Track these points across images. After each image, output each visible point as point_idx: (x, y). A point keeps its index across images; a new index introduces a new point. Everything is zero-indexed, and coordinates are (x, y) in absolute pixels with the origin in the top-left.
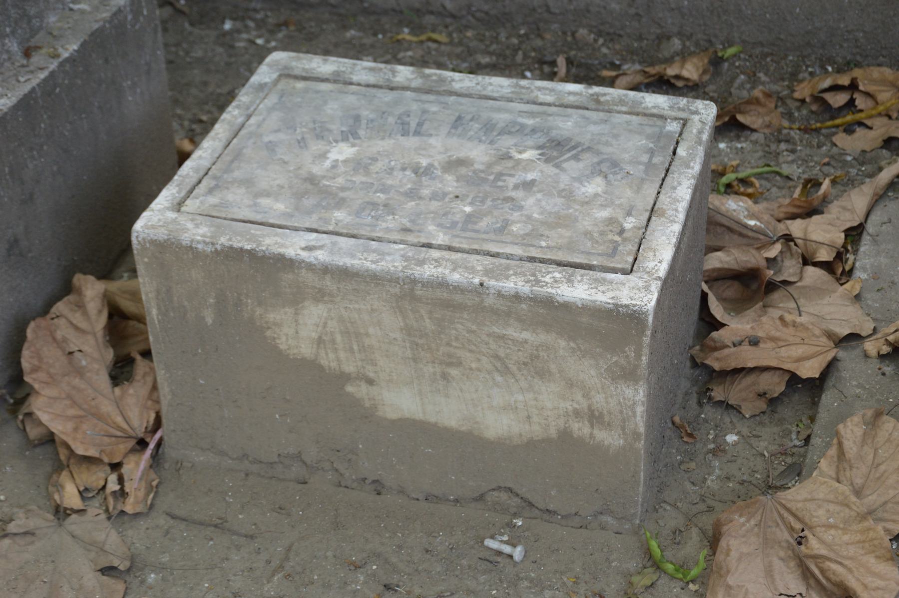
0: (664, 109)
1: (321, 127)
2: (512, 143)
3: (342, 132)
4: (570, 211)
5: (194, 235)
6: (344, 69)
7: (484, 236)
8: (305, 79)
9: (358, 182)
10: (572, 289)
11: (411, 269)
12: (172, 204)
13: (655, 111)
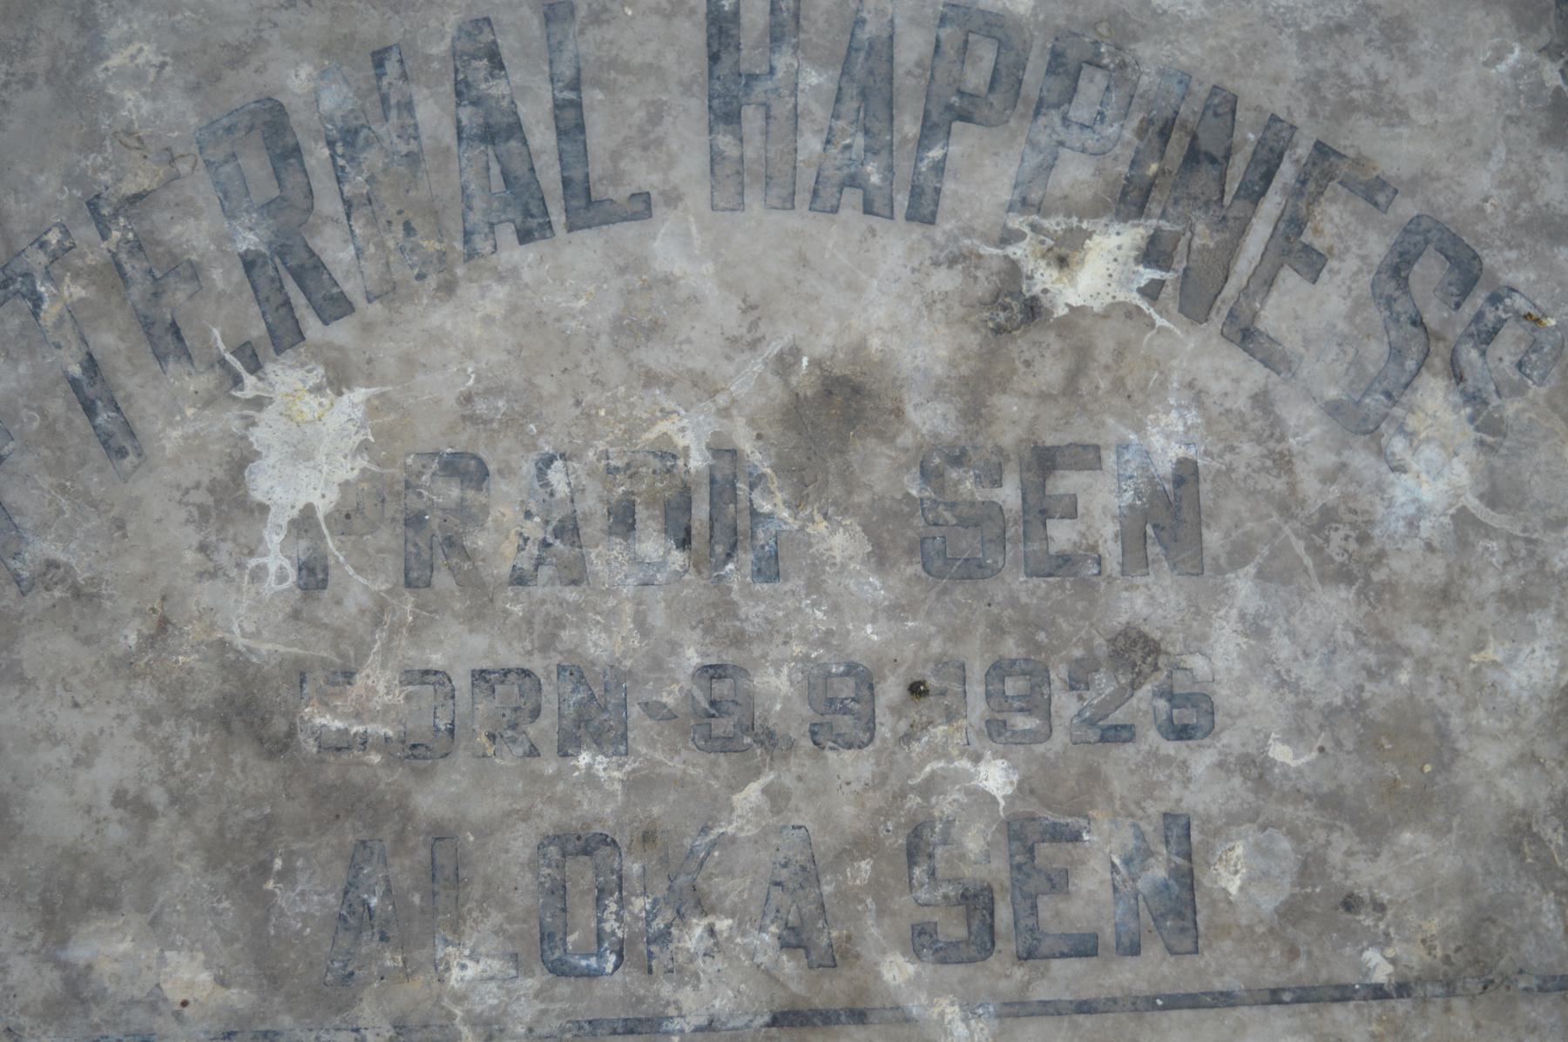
1: (137, 247)
2: (1006, 195)
3: (250, 263)
4: (1404, 678)
7: (1127, 976)
9: (462, 683)
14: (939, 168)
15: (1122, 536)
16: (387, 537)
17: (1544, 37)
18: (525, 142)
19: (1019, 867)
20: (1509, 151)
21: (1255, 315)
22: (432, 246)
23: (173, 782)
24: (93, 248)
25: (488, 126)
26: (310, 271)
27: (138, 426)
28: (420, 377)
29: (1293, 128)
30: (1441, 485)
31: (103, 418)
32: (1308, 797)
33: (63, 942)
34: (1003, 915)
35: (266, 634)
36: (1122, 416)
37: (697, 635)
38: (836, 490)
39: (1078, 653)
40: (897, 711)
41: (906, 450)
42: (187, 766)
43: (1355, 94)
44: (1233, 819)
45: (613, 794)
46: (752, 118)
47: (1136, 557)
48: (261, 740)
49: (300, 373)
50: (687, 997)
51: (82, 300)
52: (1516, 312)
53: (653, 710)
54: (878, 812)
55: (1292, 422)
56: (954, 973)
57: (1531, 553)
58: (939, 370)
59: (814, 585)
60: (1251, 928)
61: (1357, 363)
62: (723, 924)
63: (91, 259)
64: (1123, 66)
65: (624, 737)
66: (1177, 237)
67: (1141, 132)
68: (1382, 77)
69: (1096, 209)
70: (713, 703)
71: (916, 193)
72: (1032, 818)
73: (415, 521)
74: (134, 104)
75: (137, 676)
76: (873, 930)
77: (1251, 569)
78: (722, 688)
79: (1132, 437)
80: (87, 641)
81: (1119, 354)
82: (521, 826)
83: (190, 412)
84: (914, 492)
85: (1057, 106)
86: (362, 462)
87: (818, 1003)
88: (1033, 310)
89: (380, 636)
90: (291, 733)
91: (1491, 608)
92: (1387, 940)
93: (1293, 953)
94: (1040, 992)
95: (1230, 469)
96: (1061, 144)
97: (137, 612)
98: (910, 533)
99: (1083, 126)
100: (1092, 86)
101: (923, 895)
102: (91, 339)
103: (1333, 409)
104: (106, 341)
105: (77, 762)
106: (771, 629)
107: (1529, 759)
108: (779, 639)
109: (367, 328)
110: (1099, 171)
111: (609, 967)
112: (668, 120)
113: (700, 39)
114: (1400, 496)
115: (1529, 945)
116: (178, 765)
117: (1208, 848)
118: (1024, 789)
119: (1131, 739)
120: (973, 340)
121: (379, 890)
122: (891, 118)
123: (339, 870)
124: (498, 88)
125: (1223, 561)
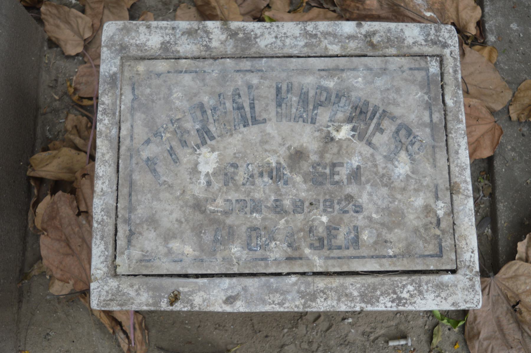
0: (421, 45)
1: (179, 128)
2: (328, 119)
3: (198, 131)
4: (396, 203)
5: (140, 304)
6: (167, 39)
7: (347, 253)
8: (143, 59)
9: (234, 202)
10: (423, 302)
11: (309, 307)
12: (108, 267)
13: (416, 49)
14: (316, 114)
15: (347, 178)
16: (221, 177)
17: (425, 91)
18: (244, 110)
19: (328, 234)
20: (418, 111)
21: (371, 140)
22: (229, 128)
23: (186, 217)
24: (171, 128)
25: (238, 107)
26: (208, 132)
27: (179, 158)
28: (227, 150)
29: (379, 107)
30: (404, 170)
31: (173, 157)
32: (379, 223)
33: (168, 244)
34: (326, 242)
35: (201, 193)
36: (347, 158)
37: (274, 194)
38: (298, 170)
39: (339, 198)
40: (308, 207)
41: (310, 163)
42: (188, 215)
43: (390, 101)
44: (366, 227)
45: (259, 221)
46: (284, 106)
47: (349, 182)
48: (200, 211)
49: (207, 149)
50: (272, 255)
51: (170, 137)
52: (418, 140)
53: (266, 207)
54: (304, 224)
55: (377, 159)
56: (317, 252)
57: (420, 182)
58: (316, 149)
59: (294, 186)
60: (368, 245)
61: (389, 149)
62: (278, 243)
63: (171, 130)
64: (349, 96)
65: (261, 211)
66: (358, 126)
67: (352, 108)
68: (395, 98)
69: (344, 122)
70: (276, 206)
71: (312, 119)
72: (331, 226)
73: (226, 174)
74: (178, 103)
75: (179, 200)
76: (303, 244)
77: (370, 184)
78: (278, 203)
79: (349, 161)
80: (171, 194)
81: (347, 147)
82: (244, 226)
83: (188, 156)
84: (311, 170)
85: (337, 103)
86: (217, 164)
87: (294, 256)
88: (332, 139)
89: (220, 194)
90: (205, 210)
91: (412, 191)
92: (392, 248)
93: (376, 250)
94: (332, 255)
95: (366, 167)
96: (338, 110)
97: (179, 189)
98: (310, 177)
99: (342, 107)
100: (343, 100)
101: (312, 239)
102: (171, 143)
103: (385, 157)
104: (174, 144)
105: (170, 214)
106: (286, 193)
107: (418, 218)
108: (288, 195)
109: (218, 142)
110: (344, 115)
111: (259, 249)
112: (269, 106)
113: (275, 92)
114: (396, 172)
115: (417, 250)
116: (186, 215)
117: (361, 232)
118: (329, 221)
119: (348, 213)
120: (321, 144)
121: (220, 236)
122: (308, 106)
123: (213, 233)
124: (240, 101)
125: (365, 183)
